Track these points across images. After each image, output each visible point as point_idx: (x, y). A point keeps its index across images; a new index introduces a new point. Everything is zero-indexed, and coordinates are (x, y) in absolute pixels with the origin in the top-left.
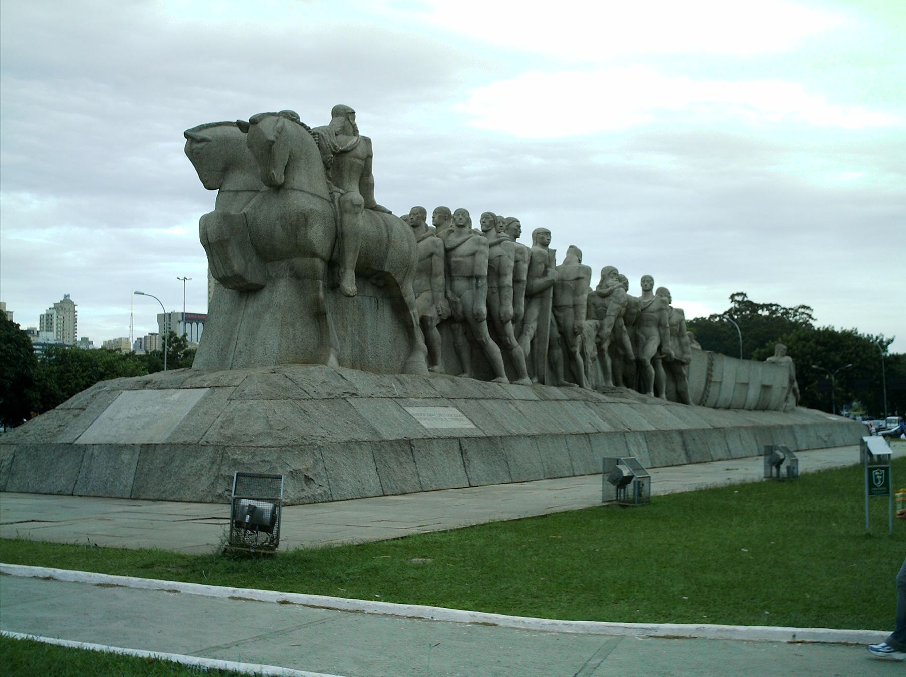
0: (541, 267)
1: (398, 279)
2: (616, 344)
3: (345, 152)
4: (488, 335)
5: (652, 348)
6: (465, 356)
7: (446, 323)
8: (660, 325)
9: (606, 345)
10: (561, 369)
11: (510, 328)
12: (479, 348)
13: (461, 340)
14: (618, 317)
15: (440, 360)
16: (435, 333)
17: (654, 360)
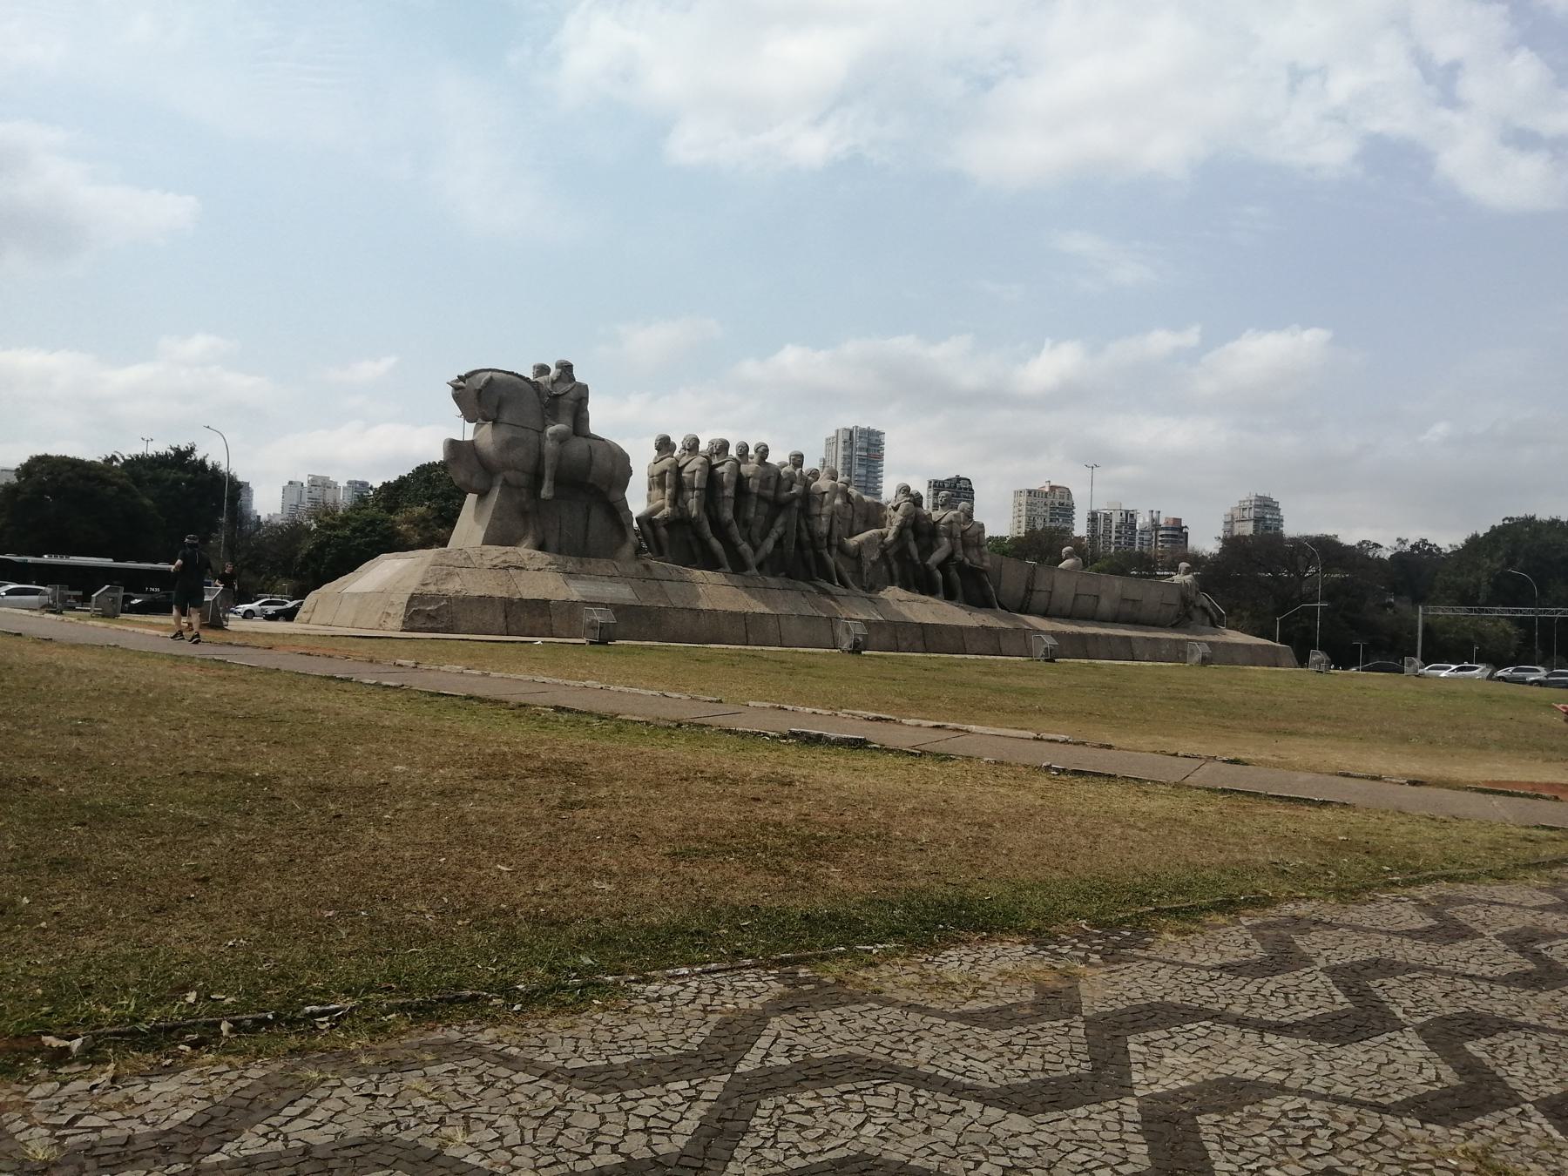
0: (787, 483)
1: (605, 488)
2: (902, 554)
3: (557, 396)
4: (710, 534)
5: (937, 556)
6: (696, 550)
7: (670, 523)
8: (951, 536)
9: (890, 552)
10: (814, 568)
11: (734, 529)
12: (704, 543)
13: (691, 537)
14: (901, 528)
15: (666, 551)
16: (663, 532)
17: (942, 566)
